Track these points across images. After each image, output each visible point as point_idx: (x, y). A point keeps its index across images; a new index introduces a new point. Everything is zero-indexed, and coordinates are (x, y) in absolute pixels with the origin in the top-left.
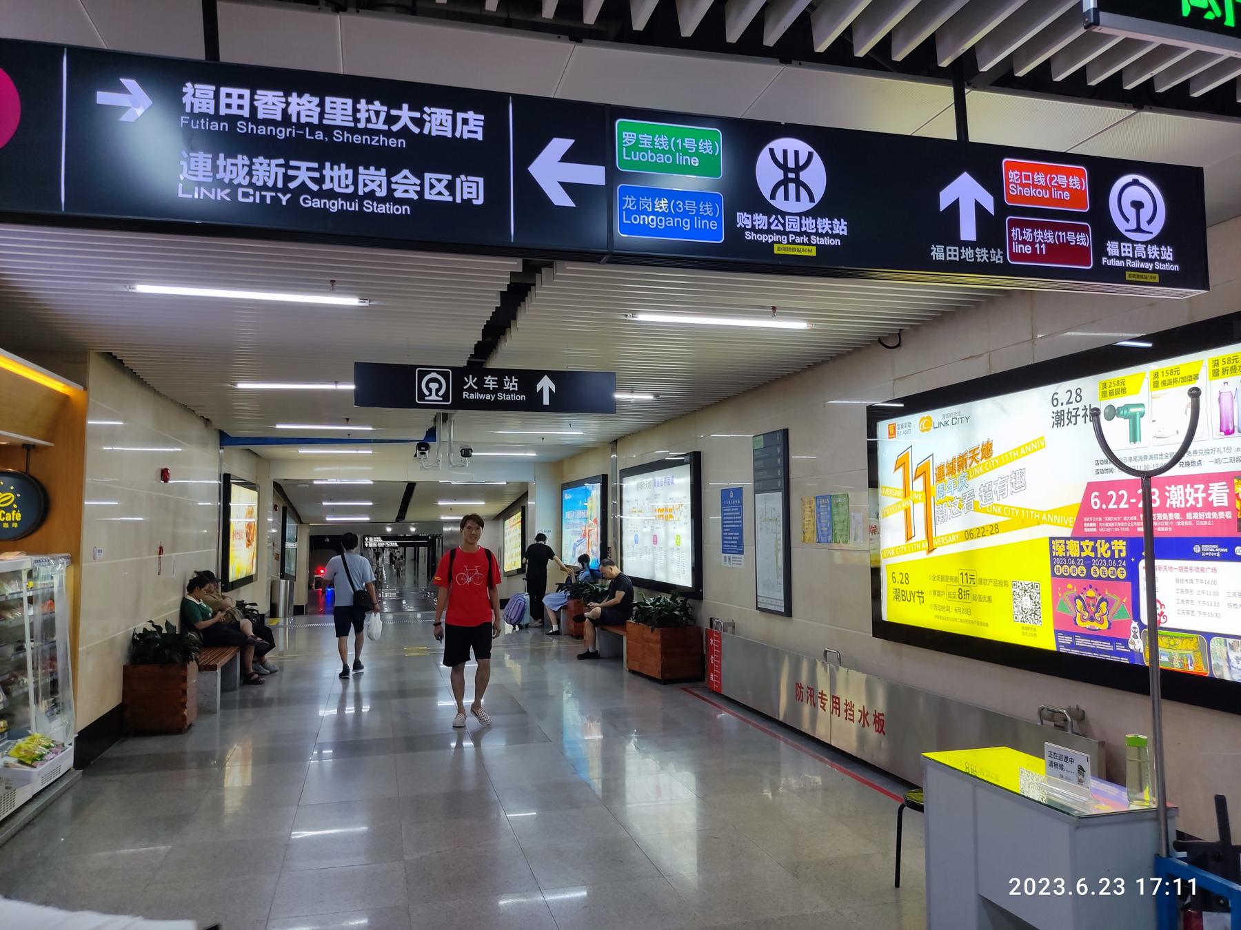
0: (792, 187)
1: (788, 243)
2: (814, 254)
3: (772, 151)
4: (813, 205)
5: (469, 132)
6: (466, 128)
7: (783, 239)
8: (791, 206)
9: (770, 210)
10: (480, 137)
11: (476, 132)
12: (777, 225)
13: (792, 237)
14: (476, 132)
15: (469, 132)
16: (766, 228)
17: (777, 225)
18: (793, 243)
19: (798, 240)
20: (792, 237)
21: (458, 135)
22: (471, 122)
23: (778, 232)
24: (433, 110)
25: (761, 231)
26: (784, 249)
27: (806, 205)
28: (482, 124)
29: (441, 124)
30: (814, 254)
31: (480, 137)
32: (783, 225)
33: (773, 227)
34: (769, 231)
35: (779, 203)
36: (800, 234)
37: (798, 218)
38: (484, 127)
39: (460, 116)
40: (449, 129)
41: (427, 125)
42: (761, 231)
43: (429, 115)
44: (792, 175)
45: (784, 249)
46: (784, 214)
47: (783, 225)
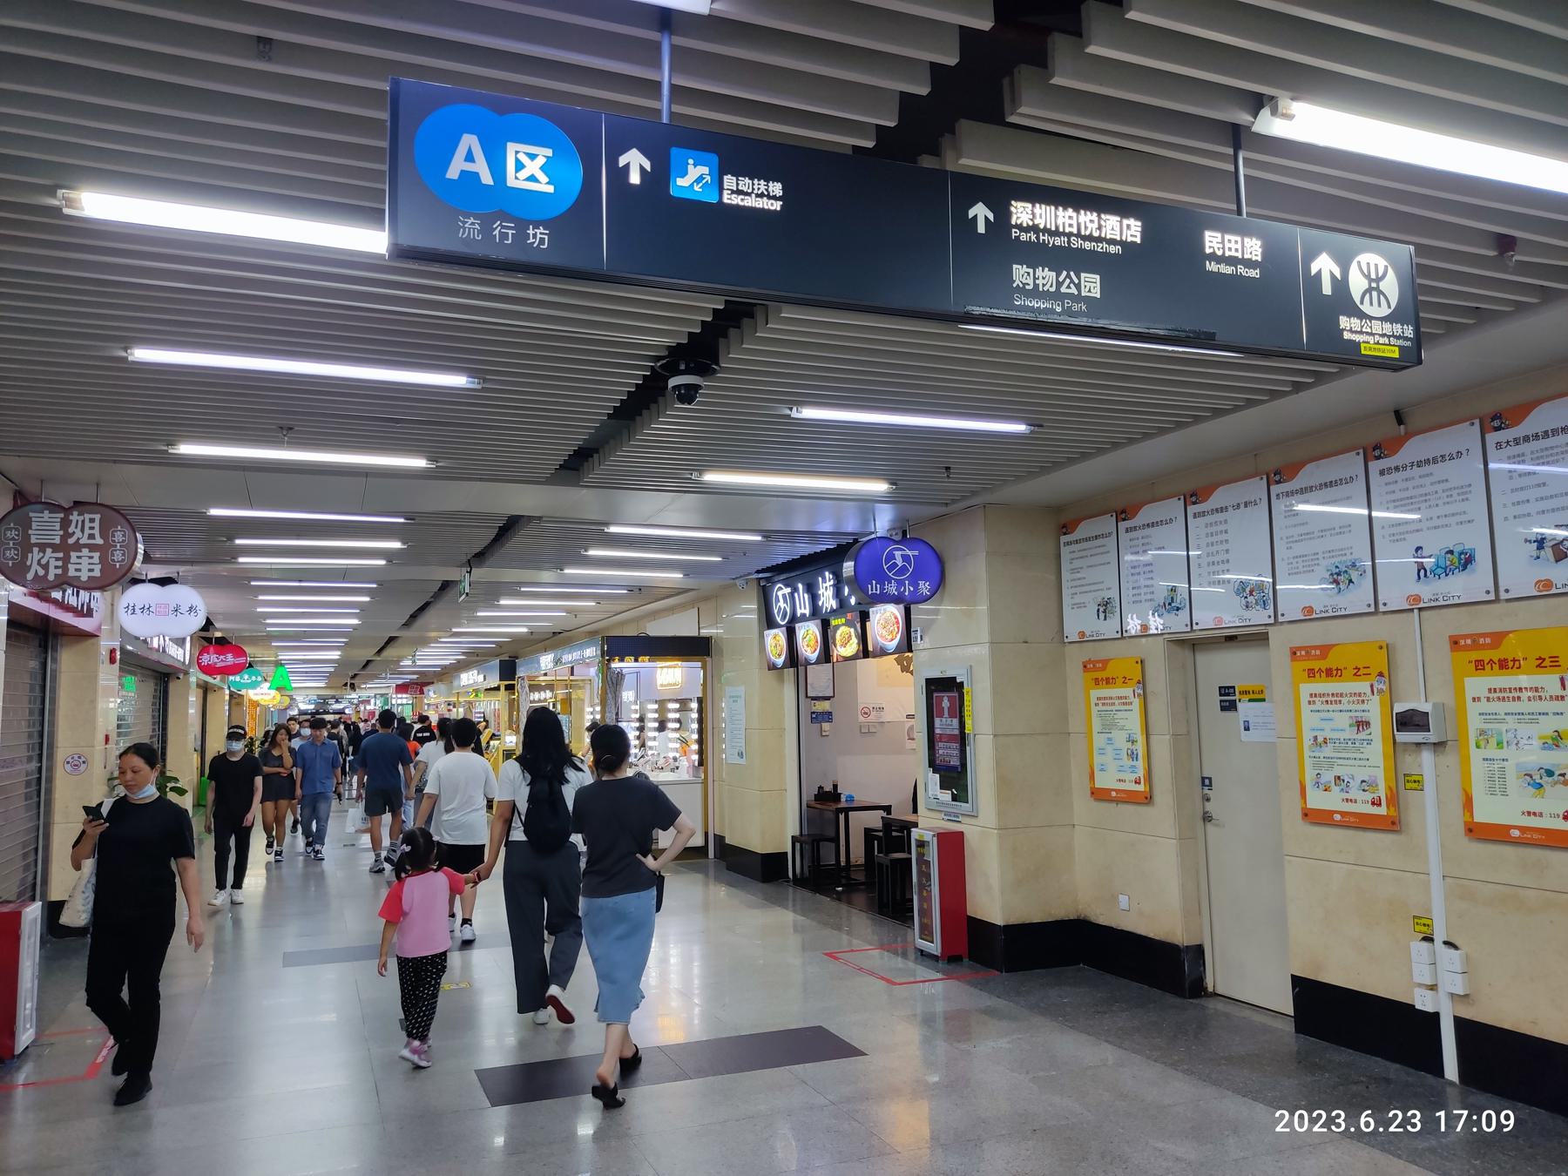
2: (1396, 355)
3: (1359, 263)
4: (1390, 311)
5: (1131, 236)
6: (1129, 233)
10: (1138, 240)
11: (1136, 236)
14: (1136, 236)
15: (1131, 236)
16: (1359, 330)
21: (1124, 239)
22: (1133, 228)
23: (1367, 333)
24: (1108, 217)
25: (1356, 332)
26: (1370, 349)
27: (1385, 311)
28: (1139, 229)
29: (1113, 229)
30: (1396, 355)
31: (1138, 240)
33: (1364, 330)
34: (1361, 332)
35: (1366, 308)
36: (1383, 335)
38: (1141, 232)
39: (1125, 222)
40: (1118, 233)
41: (1104, 230)
42: (1356, 332)
43: (1105, 221)
44: (1374, 285)
45: (1370, 349)
46: (1371, 318)
47: (1371, 327)
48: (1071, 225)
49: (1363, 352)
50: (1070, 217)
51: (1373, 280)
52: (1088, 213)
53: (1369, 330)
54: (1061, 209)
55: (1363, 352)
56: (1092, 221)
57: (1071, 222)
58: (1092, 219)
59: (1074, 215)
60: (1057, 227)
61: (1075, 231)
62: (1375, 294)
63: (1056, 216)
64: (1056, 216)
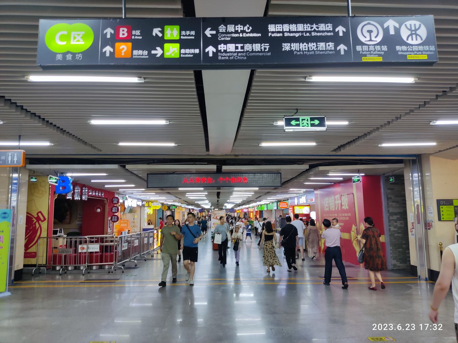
0: (414, 36)
1: (414, 54)
7: (413, 53)
8: (414, 42)
9: (407, 45)
12: (410, 49)
13: (415, 53)
17: (410, 49)
18: (416, 54)
19: (418, 53)
20: (415, 53)
23: (410, 51)
32: (412, 49)
33: (409, 50)
37: (417, 46)
44: (413, 32)
45: (411, 57)
46: (412, 45)
47: (412, 49)
48: (305, 48)
49: (408, 58)
50: (305, 46)
51: (413, 31)
52: (312, 43)
53: (411, 50)
54: (301, 43)
55: (408, 58)
56: (314, 46)
57: (305, 47)
58: (314, 45)
59: (307, 45)
60: (300, 49)
61: (307, 49)
62: (414, 36)
63: (300, 46)
64: (300, 46)
